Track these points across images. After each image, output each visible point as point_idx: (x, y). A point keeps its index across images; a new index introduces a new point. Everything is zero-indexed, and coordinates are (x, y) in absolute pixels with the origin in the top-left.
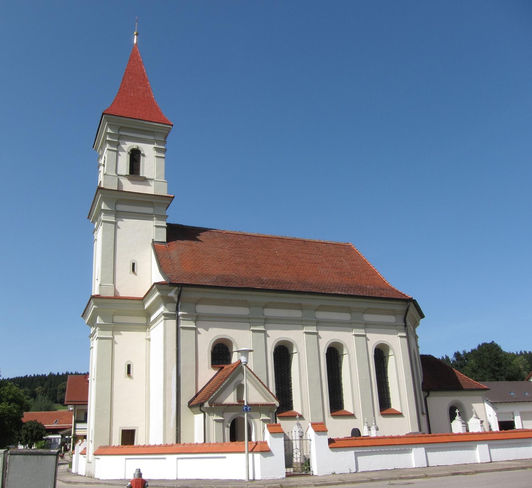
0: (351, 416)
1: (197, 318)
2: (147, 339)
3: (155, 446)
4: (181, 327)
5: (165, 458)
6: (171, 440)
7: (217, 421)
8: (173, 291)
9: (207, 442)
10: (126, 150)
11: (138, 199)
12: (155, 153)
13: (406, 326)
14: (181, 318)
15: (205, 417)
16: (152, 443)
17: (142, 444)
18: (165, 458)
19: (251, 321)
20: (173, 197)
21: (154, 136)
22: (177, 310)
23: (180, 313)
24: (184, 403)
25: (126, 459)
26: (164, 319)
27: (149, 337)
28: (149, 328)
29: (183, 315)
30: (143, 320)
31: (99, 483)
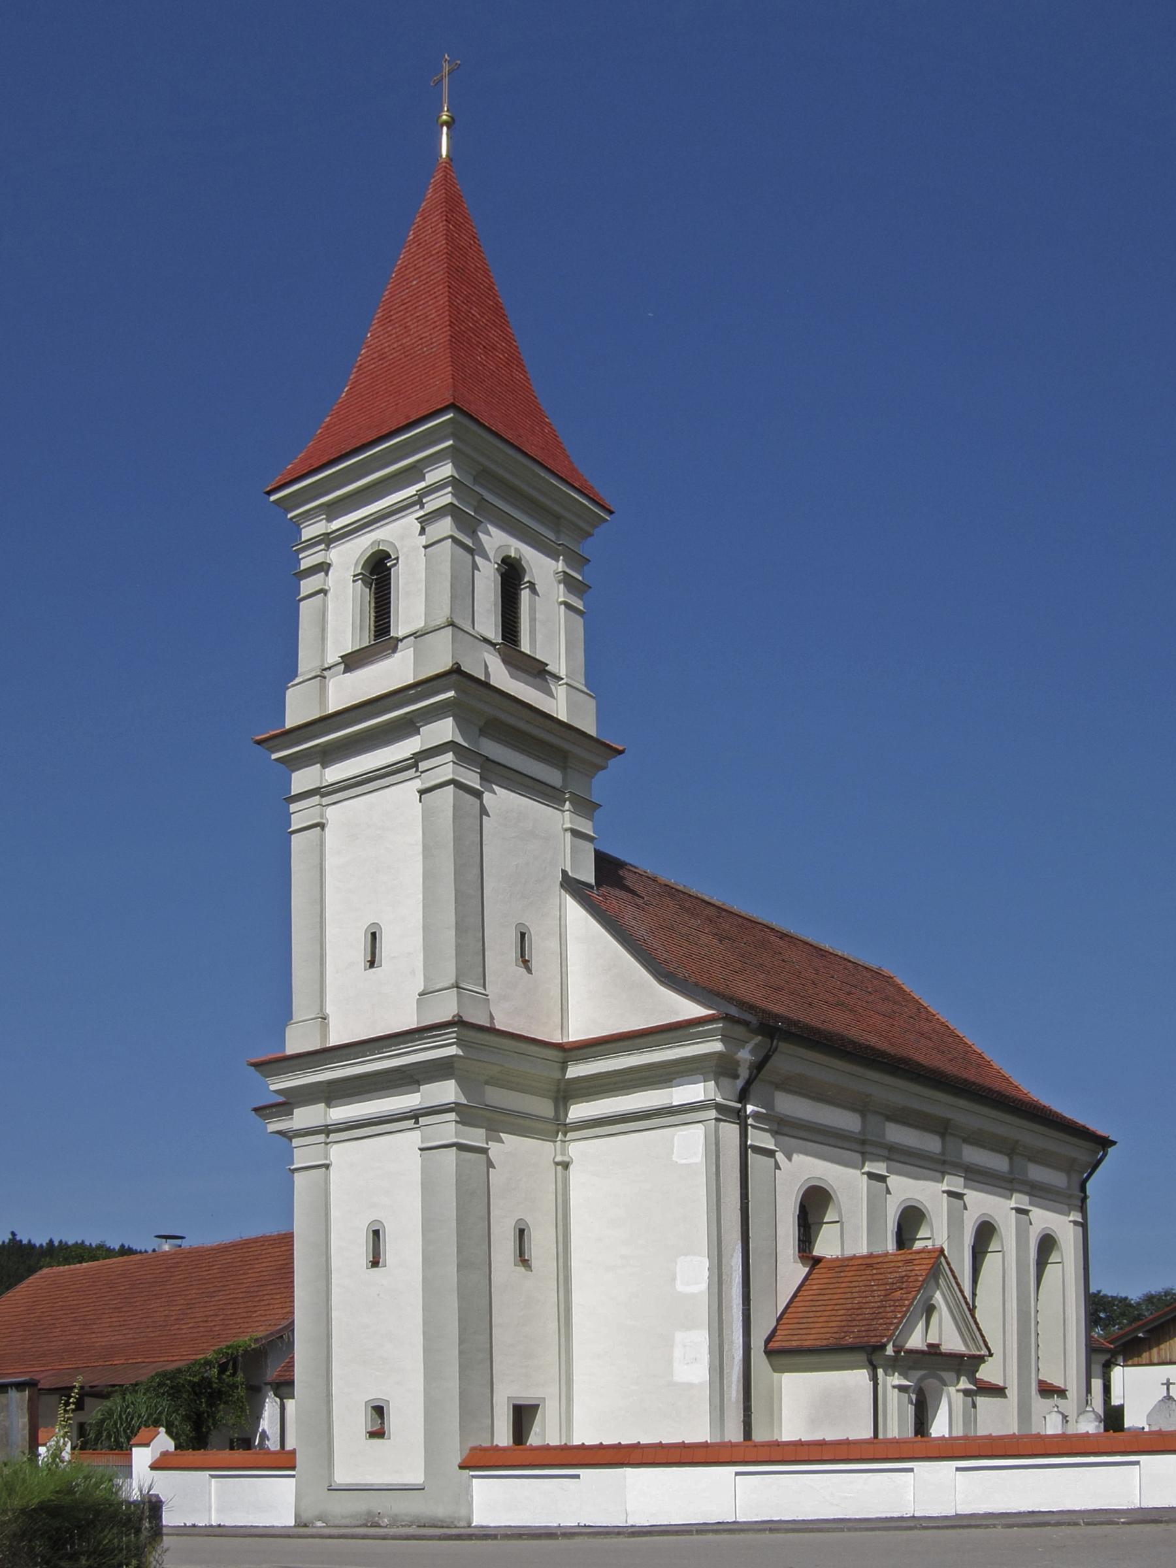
0: (958, 1391)
1: (781, 1126)
2: (557, 1164)
3: (583, 1447)
4: (752, 1146)
5: (578, 1477)
6: (734, 1434)
7: (902, 1389)
8: (749, 1046)
9: (881, 1436)
10: (491, 555)
11: (536, 732)
12: (561, 592)
13: (1084, 1199)
14: (750, 1121)
15: (875, 1379)
16: (576, 1441)
17: (554, 1440)
18: (578, 1477)
19: (868, 1149)
20: (621, 752)
21: (557, 532)
22: (743, 1097)
23: (750, 1108)
24: (758, 1344)
25: (737, 1474)
26: (717, 1120)
27: (566, 1159)
28: (565, 1135)
29: (756, 1115)
30: (545, 1108)
31: (494, 1537)
